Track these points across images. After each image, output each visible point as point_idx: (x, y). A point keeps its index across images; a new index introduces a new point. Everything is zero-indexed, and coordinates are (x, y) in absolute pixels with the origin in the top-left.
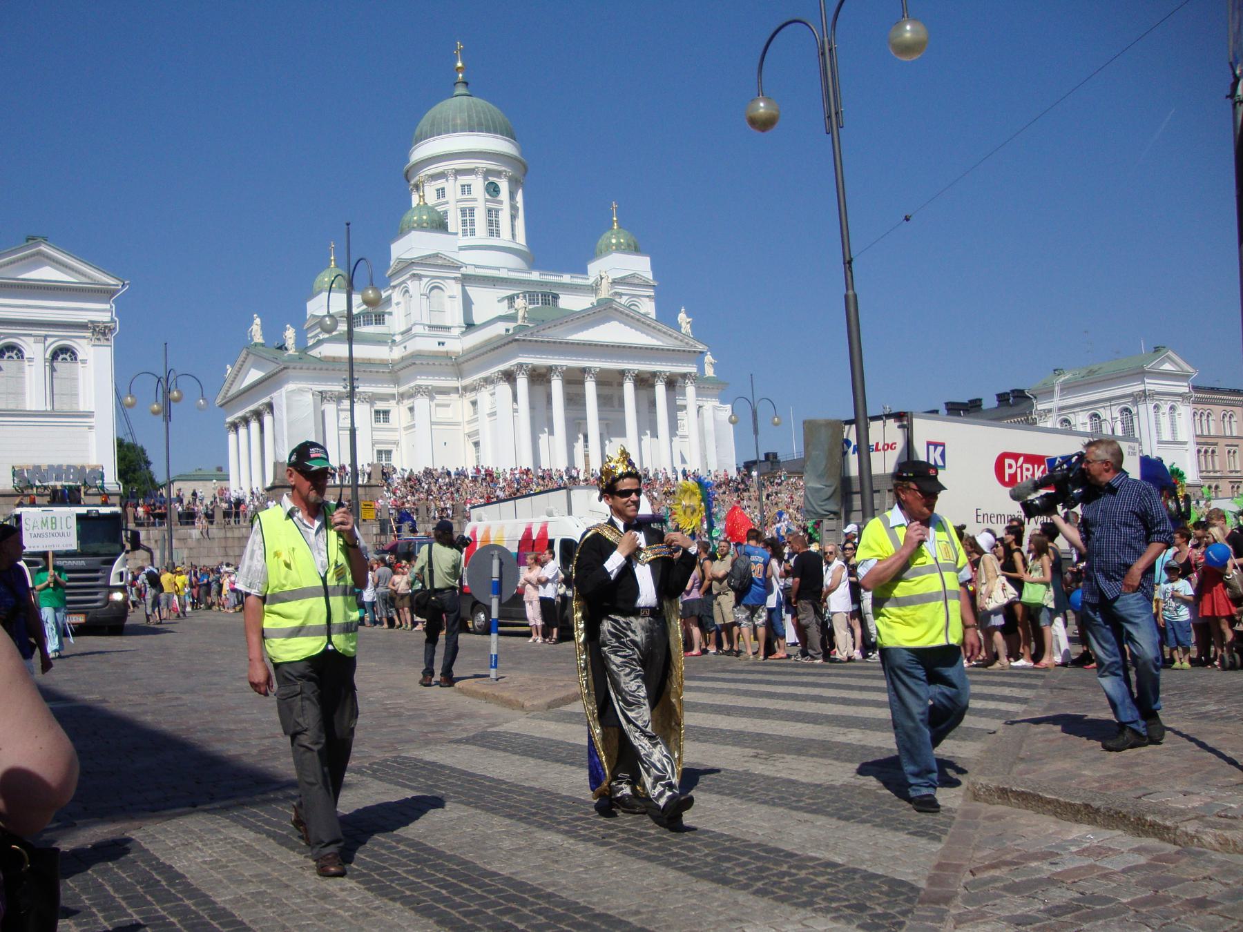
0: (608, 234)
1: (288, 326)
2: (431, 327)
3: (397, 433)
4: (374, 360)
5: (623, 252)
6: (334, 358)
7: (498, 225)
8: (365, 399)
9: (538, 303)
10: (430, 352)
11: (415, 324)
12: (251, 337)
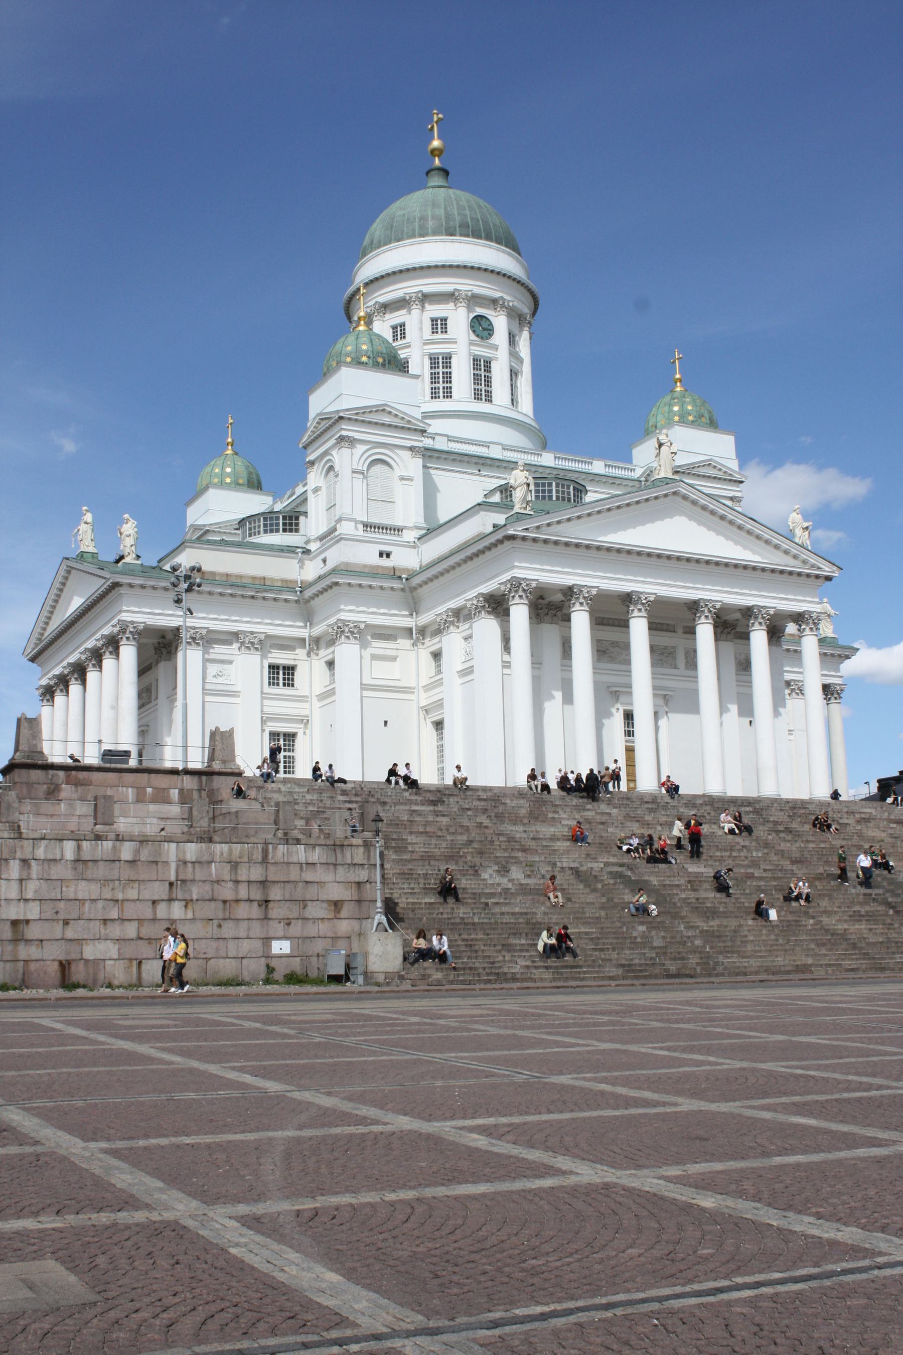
0: (667, 399)
1: (126, 516)
2: (366, 525)
3: (307, 705)
5: (694, 424)
8: (253, 643)
9: (550, 497)
10: (365, 566)
11: (340, 520)
12: (76, 540)
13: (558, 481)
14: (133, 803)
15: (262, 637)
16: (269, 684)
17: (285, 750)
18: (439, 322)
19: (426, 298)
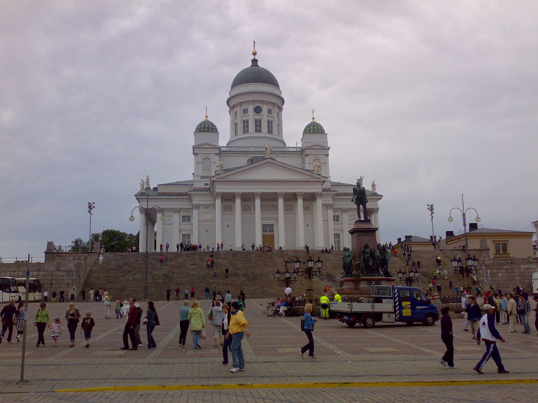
2: (202, 177)
7: (260, 126)
13: (261, 157)
14: (72, 260)
15: (179, 209)
16: (183, 222)
17: (186, 239)
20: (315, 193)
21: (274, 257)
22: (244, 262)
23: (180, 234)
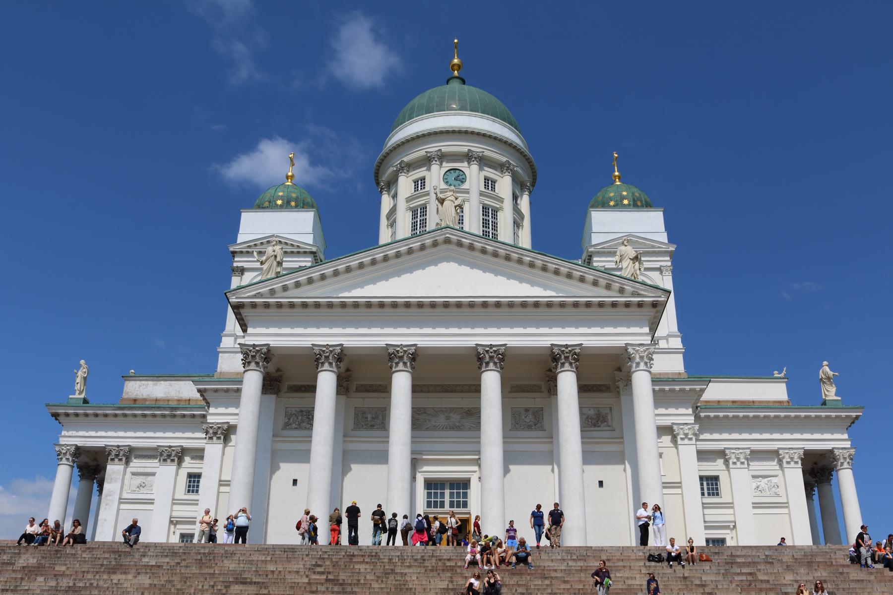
4: (197, 400)
6: (135, 400)
16: (189, 491)
18: (420, 182)
19: (409, 167)
20: (625, 348)
21: (406, 571)
22: (236, 589)
23: (174, 532)
